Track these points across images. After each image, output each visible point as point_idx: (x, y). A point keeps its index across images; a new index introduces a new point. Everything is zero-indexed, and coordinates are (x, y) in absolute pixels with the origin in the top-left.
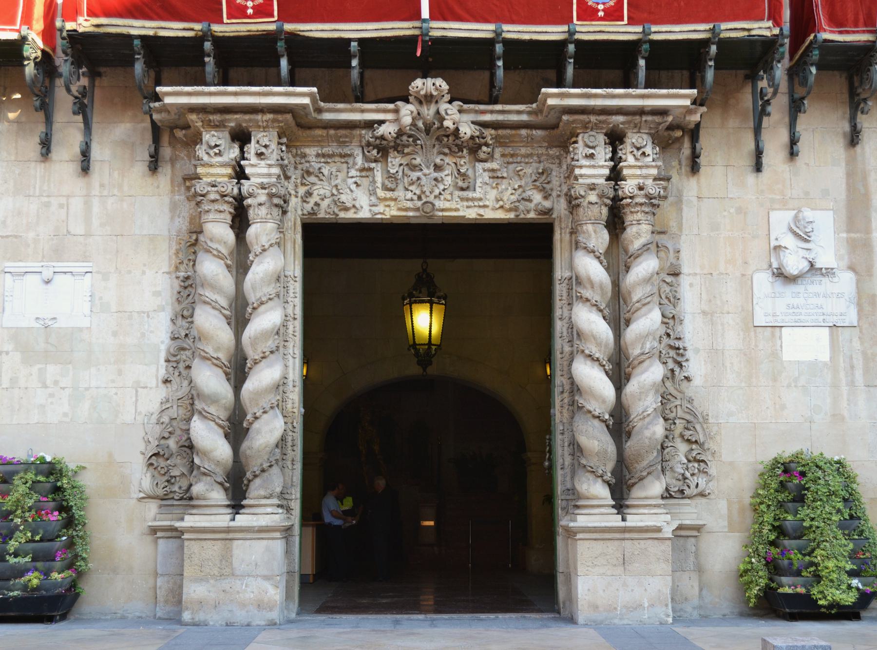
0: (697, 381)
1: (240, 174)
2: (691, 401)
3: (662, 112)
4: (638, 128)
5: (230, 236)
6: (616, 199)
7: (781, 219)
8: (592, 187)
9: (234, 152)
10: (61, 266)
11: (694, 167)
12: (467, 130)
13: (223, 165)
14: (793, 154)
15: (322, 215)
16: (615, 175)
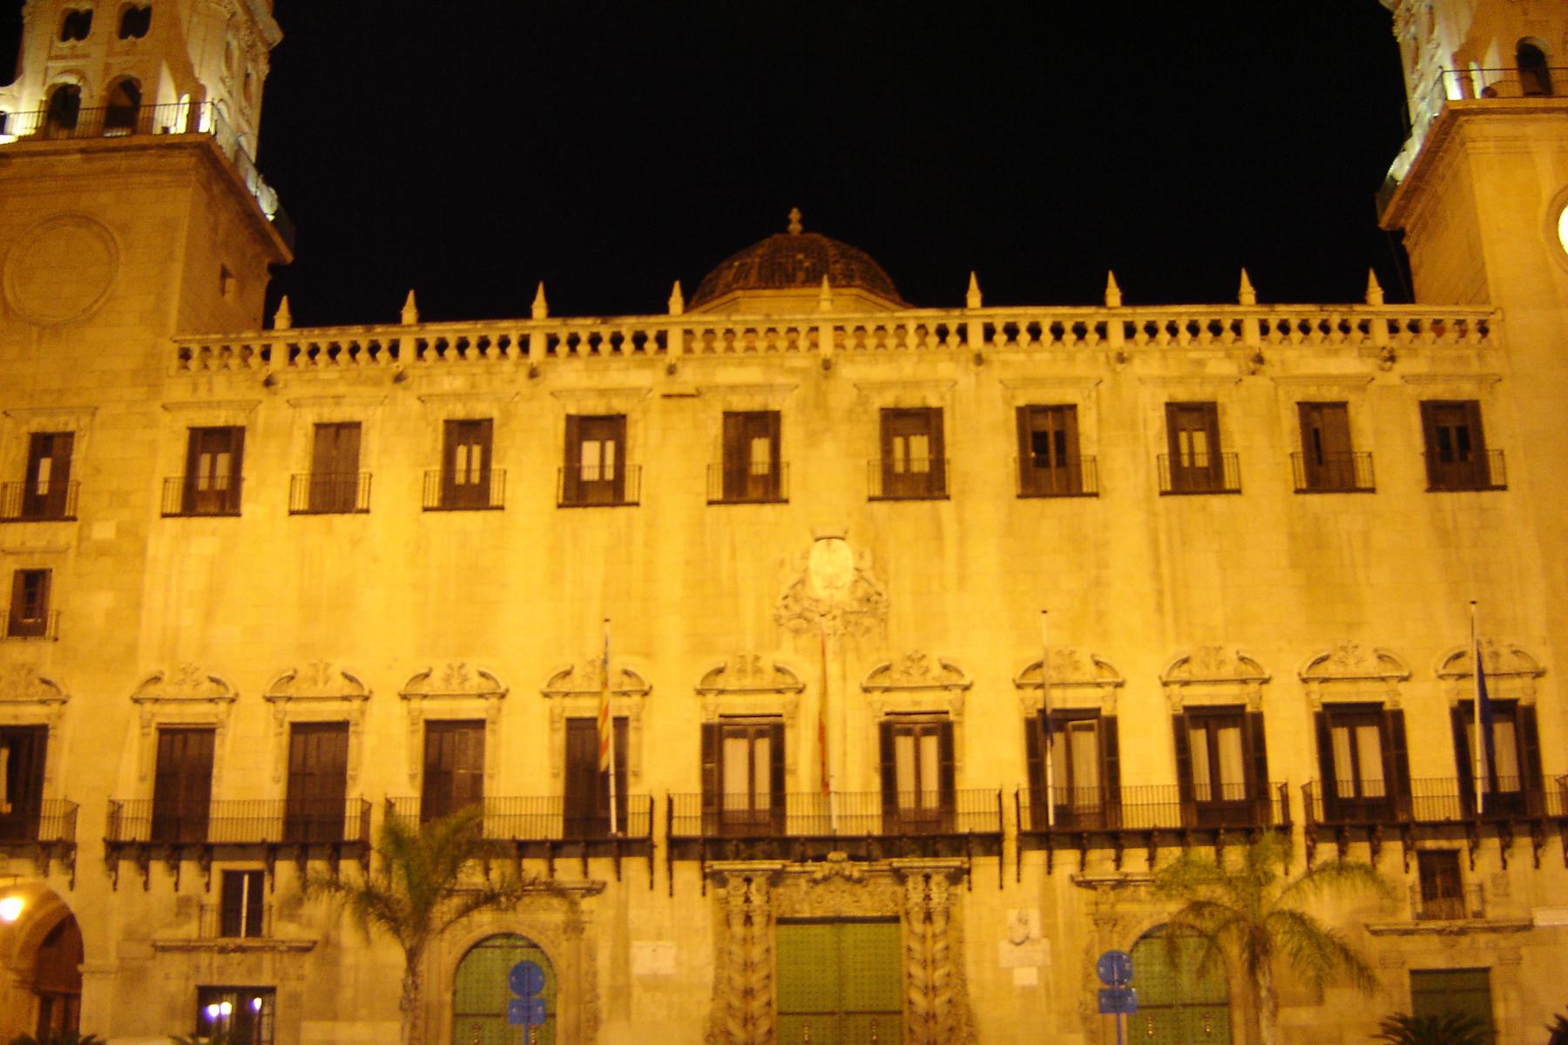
1: (747, 900)
4: (938, 873)
7: (1012, 915)
9: (744, 889)
10: (660, 943)
12: (856, 874)
13: (740, 896)
15: (786, 916)
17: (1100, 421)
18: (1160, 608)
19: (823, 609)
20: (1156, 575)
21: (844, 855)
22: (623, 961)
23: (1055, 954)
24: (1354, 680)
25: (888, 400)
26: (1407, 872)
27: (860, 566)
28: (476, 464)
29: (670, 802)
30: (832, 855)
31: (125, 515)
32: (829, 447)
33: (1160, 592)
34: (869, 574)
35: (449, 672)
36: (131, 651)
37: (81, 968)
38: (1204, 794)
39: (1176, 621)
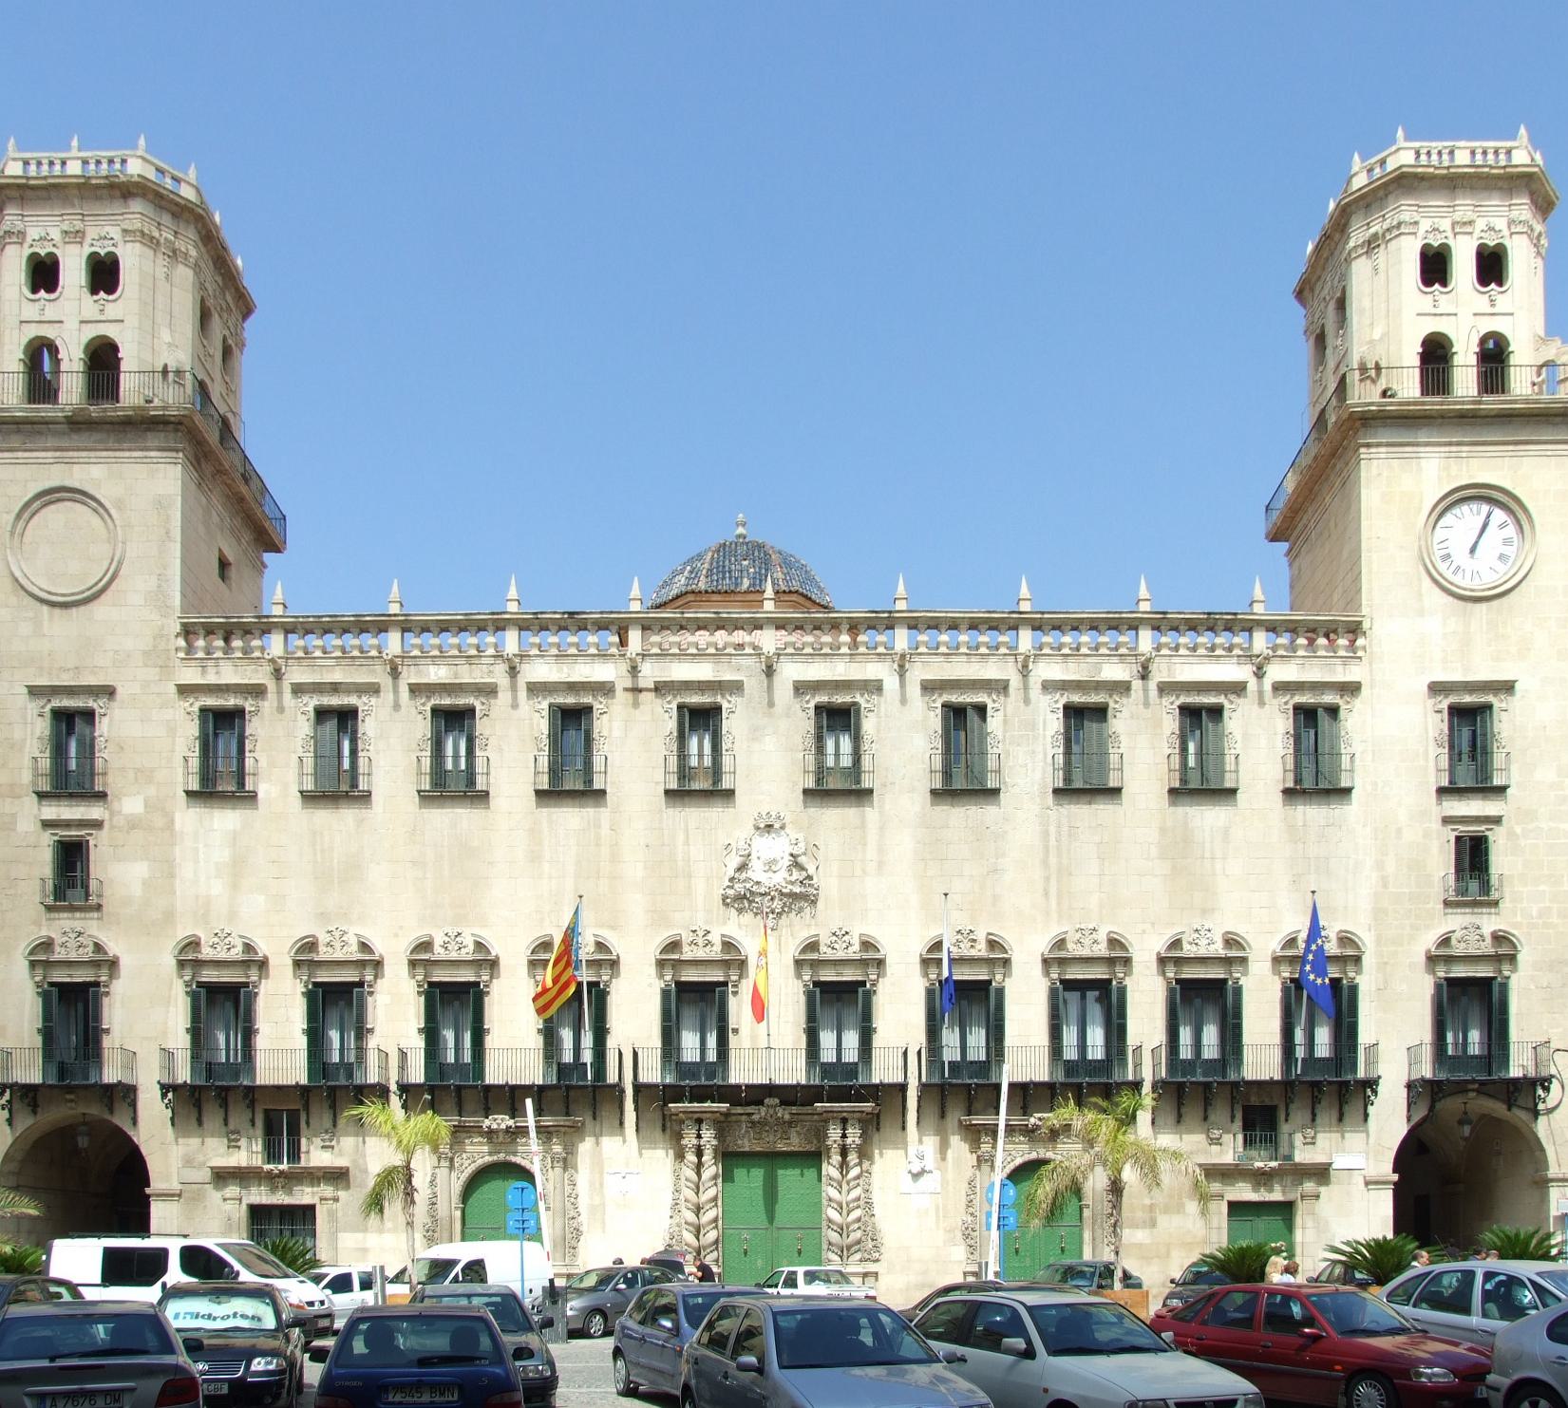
5: (695, 1160)
6: (844, 1145)
8: (835, 1141)
11: (878, 1129)
12: (787, 1117)
16: (844, 1136)
17: (1005, 722)
18: (1046, 894)
19: (762, 890)
20: (1045, 863)
21: (777, 1101)
23: (944, 1182)
27: (794, 852)
28: (463, 752)
29: (635, 1054)
31: (152, 791)
32: (770, 743)
33: (1047, 879)
35: (447, 939)
36: (169, 917)
37: (148, 1191)
38: (1070, 1053)
39: (1059, 904)
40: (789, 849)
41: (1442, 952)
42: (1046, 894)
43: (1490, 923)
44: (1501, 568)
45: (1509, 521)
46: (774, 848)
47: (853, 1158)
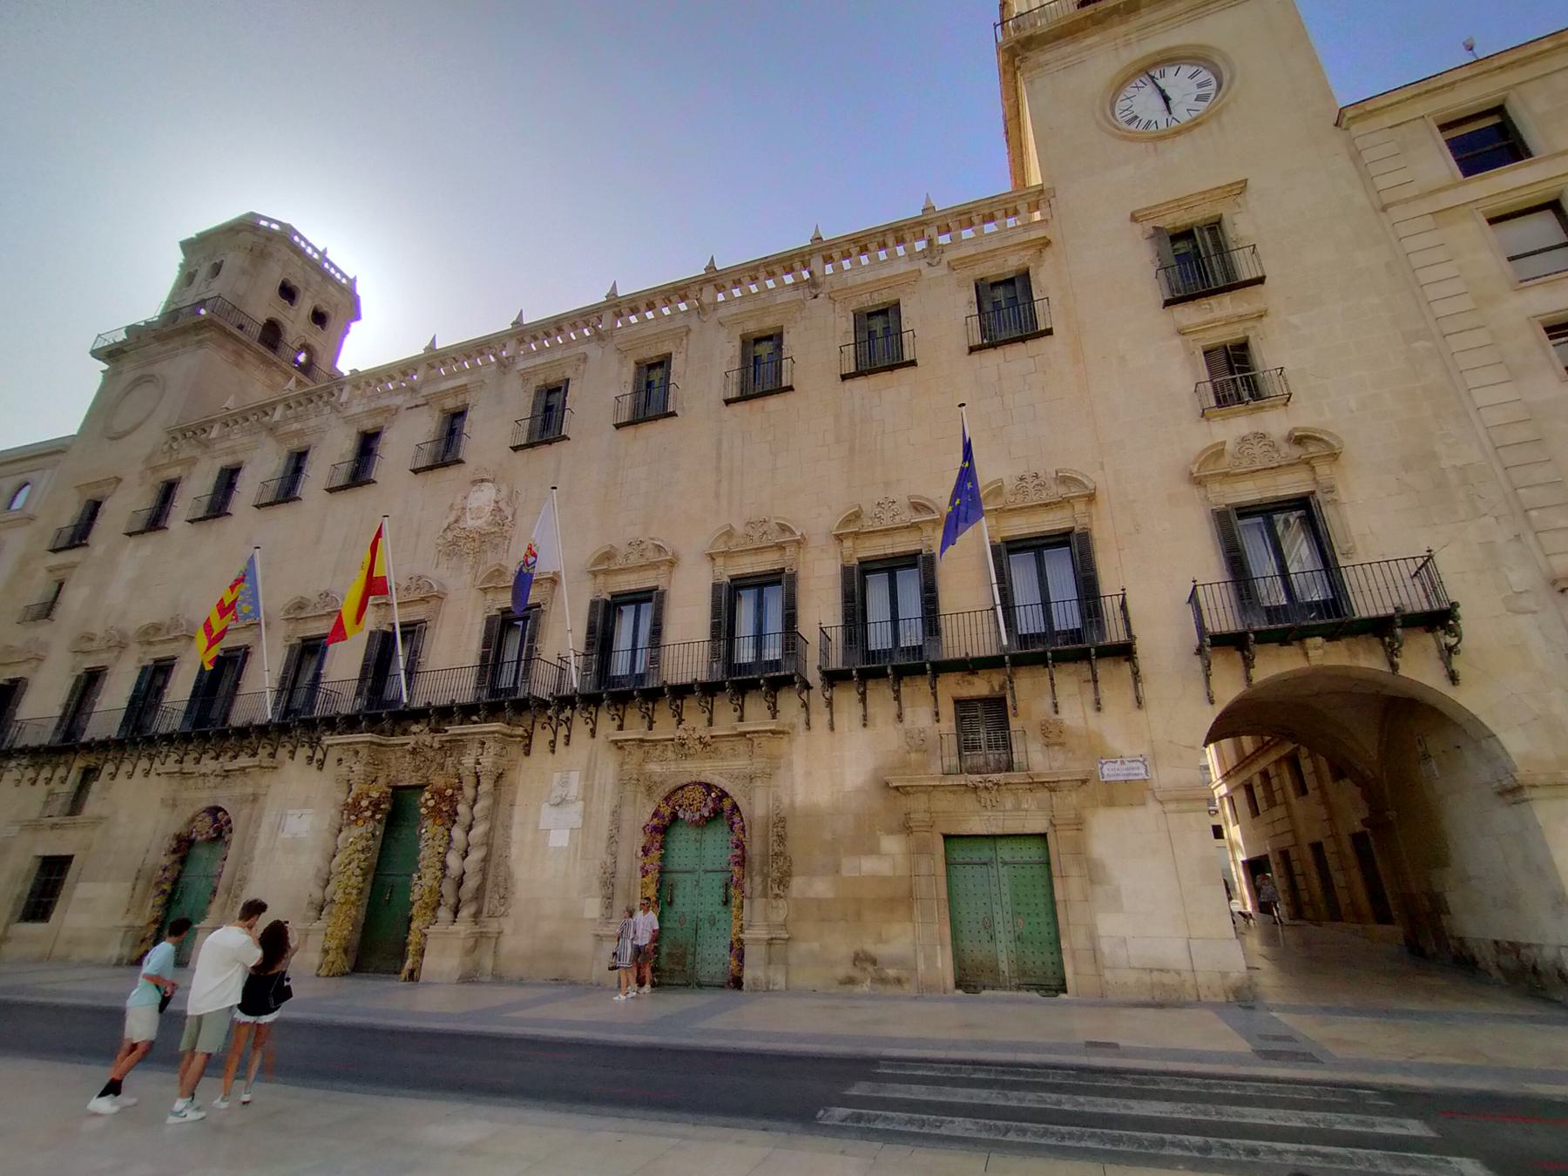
0: (513, 858)
2: (508, 867)
3: (493, 732)
10: (305, 811)
11: (527, 753)
14: (567, 744)
18: (717, 496)
20: (718, 469)
22: (279, 827)
23: (586, 815)
24: (887, 532)
25: (538, 381)
26: (938, 721)
30: (415, 728)
34: (502, 505)
40: (494, 497)
41: (1211, 469)
42: (717, 496)
43: (1275, 423)
44: (1203, 106)
45: (1201, 69)
46: (484, 497)
47: (486, 786)
